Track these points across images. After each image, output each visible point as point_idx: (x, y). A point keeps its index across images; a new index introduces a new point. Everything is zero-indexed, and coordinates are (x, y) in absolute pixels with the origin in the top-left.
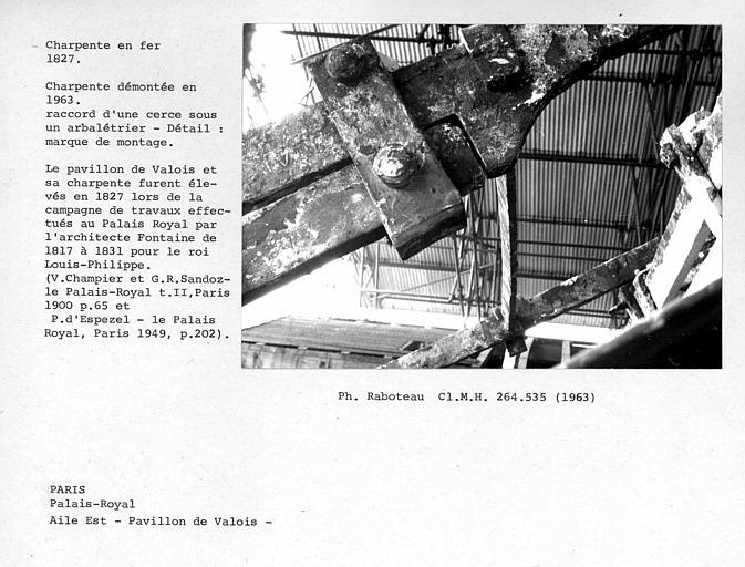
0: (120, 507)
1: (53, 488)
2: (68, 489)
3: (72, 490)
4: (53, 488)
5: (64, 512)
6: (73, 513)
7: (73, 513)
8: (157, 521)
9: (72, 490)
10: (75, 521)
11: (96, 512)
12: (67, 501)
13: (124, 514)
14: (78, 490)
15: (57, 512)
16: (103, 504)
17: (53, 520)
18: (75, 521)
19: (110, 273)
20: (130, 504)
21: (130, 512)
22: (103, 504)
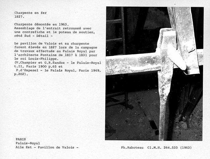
0: (36, 144)
1: (17, 139)
2: (21, 139)
3: (22, 139)
4: (17, 139)
5: (20, 145)
6: (22, 145)
7: (22, 145)
8: (46, 147)
9: (22, 139)
10: (23, 147)
11: (29, 145)
12: (21, 143)
13: (37, 146)
14: (24, 139)
15: (18, 145)
16: (31, 143)
17: (17, 147)
18: (23, 147)
19: (33, 61)
20: (38, 143)
21: (38, 145)
22: (31, 143)
